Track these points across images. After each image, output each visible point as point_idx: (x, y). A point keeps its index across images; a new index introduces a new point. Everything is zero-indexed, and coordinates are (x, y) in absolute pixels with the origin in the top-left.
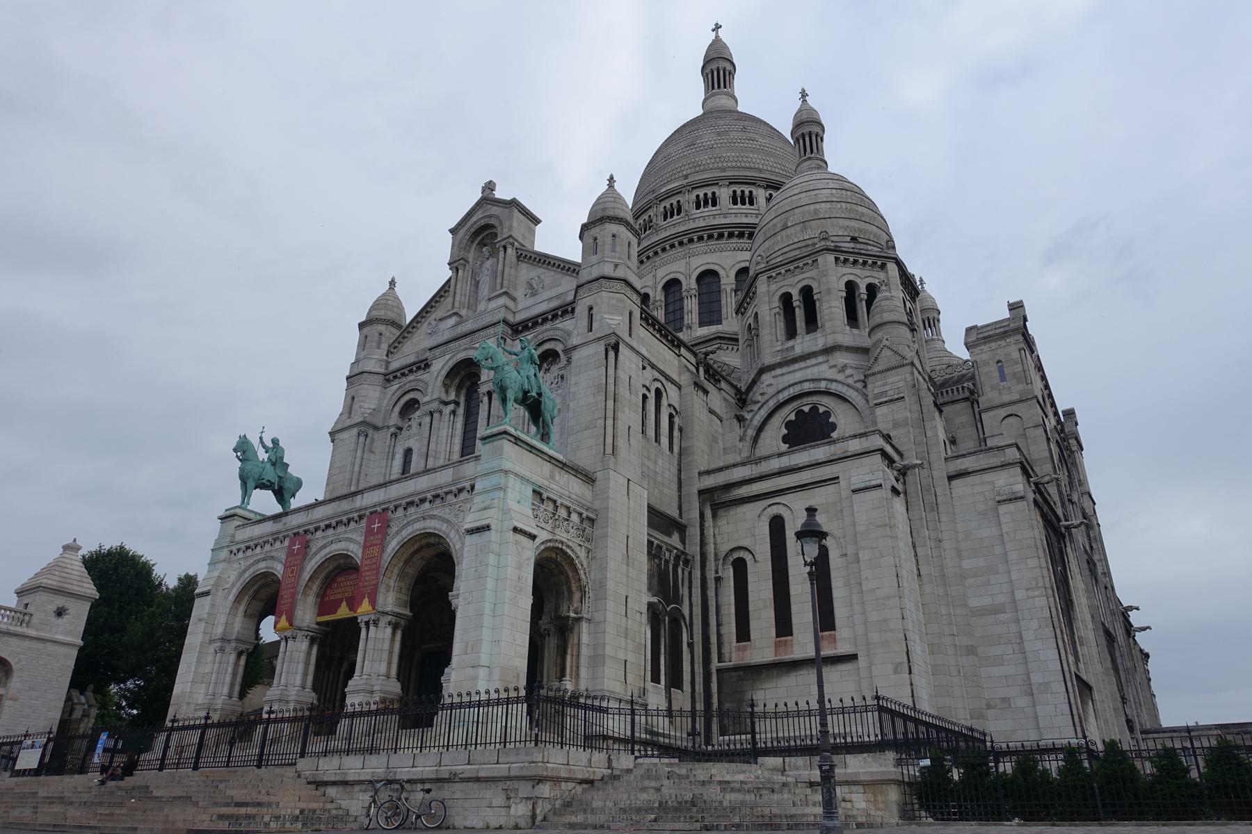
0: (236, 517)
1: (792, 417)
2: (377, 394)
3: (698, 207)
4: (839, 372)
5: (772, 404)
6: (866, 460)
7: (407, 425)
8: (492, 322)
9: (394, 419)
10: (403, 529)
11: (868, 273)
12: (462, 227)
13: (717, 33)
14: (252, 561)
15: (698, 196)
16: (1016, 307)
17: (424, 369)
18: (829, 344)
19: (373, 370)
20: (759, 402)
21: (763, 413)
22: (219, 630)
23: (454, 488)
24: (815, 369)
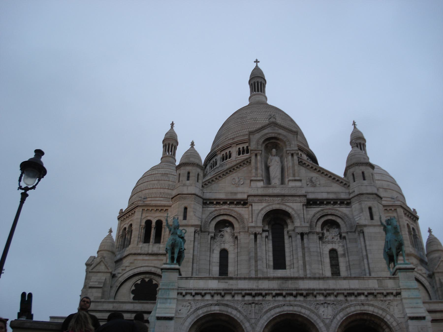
0: (178, 271)
2: (201, 210)
7: (220, 234)
8: (298, 194)
10: (347, 308)
11: (411, 222)
12: (258, 133)
13: (257, 64)
14: (202, 304)
17: (236, 205)
23: (385, 293)
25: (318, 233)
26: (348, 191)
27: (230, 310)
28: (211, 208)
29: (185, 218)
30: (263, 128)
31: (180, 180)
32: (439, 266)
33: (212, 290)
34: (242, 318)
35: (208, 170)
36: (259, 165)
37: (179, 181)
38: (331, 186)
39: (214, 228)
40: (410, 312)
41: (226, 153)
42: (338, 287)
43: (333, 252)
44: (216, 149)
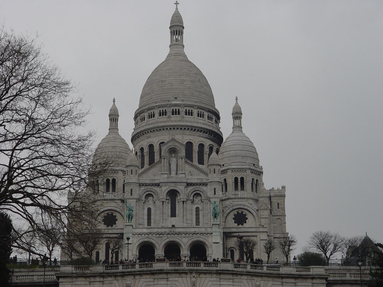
1: (236, 213)
3: (186, 115)
4: (250, 205)
5: (231, 209)
6: (264, 233)
8: (183, 182)
9: (143, 198)
15: (186, 110)
16: (284, 188)
17: (154, 186)
18: (248, 197)
19: (137, 182)
20: (228, 207)
21: (229, 211)
22: (135, 253)
24: (244, 202)
25: (191, 200)
26: (207, 178)
27: (151, 240)
28: (143, 188)
29: (131, 195)
30: (168, 142)
31: (128, 174)
32: (261, 206)
33: (145, 233)
34: (155, 243)
35: (139, 122)
36: (165, 164)
37: (127, 175)
38: (200, 175)
39: (144, 198)
40: (214, 241)
41: (151, 113)
42: (190, 231)
43: (197, 208)
44: (144, 108)
